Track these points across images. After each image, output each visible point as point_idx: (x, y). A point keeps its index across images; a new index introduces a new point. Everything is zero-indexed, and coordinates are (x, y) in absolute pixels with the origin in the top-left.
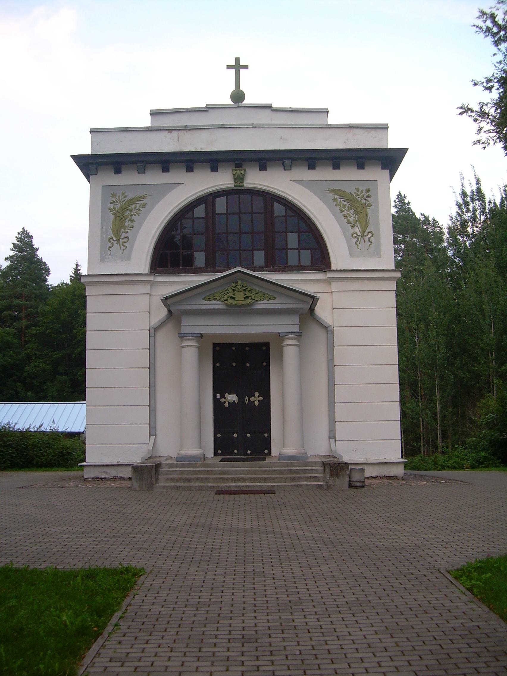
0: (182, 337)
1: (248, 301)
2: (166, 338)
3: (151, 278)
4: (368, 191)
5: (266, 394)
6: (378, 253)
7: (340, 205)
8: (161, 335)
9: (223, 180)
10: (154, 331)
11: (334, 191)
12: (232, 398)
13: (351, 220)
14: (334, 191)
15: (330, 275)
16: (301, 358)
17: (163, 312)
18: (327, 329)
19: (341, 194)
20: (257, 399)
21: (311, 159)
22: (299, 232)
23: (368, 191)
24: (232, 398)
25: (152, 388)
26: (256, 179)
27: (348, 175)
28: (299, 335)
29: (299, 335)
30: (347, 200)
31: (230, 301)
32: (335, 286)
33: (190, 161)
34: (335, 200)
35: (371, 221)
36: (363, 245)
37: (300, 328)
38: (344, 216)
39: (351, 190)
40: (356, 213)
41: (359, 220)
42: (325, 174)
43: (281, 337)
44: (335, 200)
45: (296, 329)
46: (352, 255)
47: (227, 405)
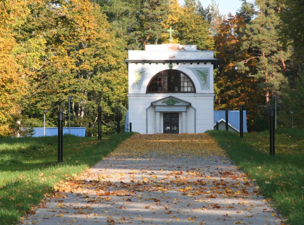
0: (156, 112)
1: (173, 103)
2: (151, 112)
3: (147, 95)
4: (207, 71)
5: (178, 127)
6: (209, 89)
7: (199, 75)
8: (149, 110)
9: (166, 67)
10: (147, 109)
11: (197, 71)
12: (169, 128)
13: (202, 79)
14: (197, 71)
15: (196, 95)
16: (186, 117)
17: (150, 104)
18: (195, 110)
19: (200, 72)
20: (175, 128)
21: (191, 62)
22: (187, 82)
23: (207, 71)
24: (169, 128)
25: (147, 125)
26: (175, 67)
27: (202, 66)
28: (186, 112)
29: (186, 112)
30: (201, 73)
31: (169, 103)
32: (197, 98)
33: (157, 62)
34: (198, 73)
35: (207, 78)
36: (205, 86)
37: (186, 110)
38: (200, 78)
39: (202, 70)
40: (204, 77)
41: (204, 79)
42: (194, 65)
43: (181, 112)
44: (198, 73)
45: (185, 110)
46: (202, 89)
47: (167, 130)
